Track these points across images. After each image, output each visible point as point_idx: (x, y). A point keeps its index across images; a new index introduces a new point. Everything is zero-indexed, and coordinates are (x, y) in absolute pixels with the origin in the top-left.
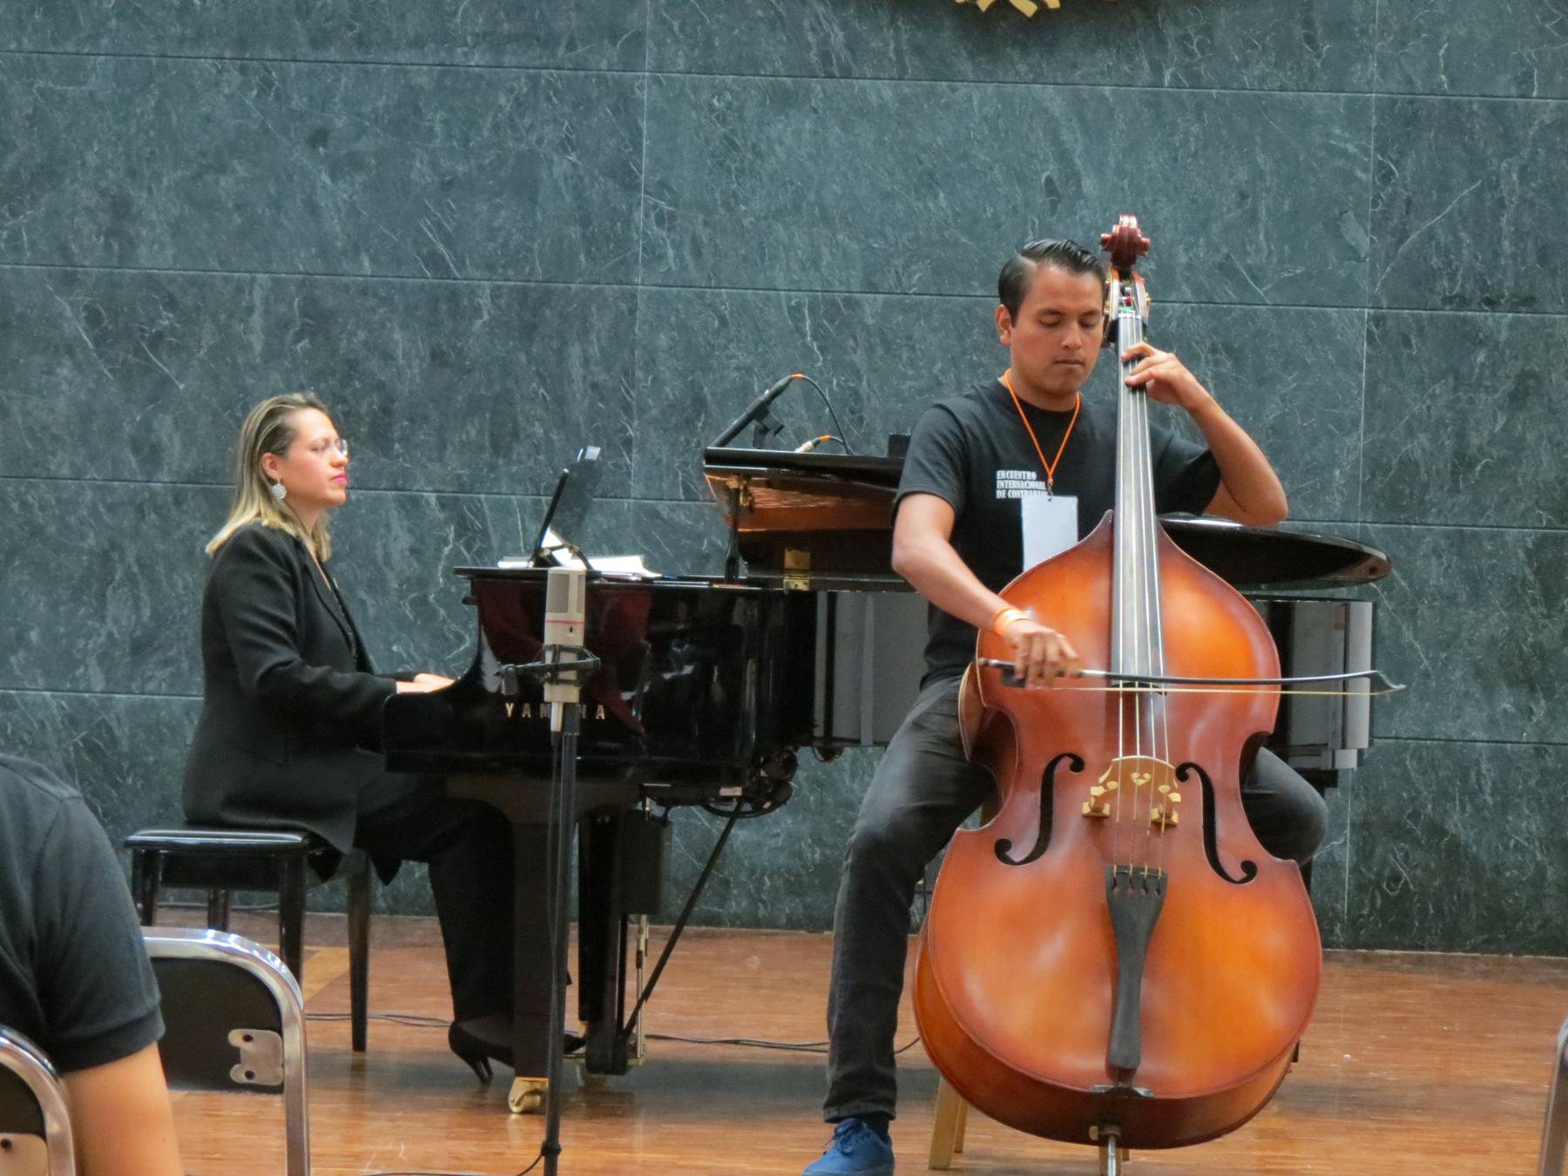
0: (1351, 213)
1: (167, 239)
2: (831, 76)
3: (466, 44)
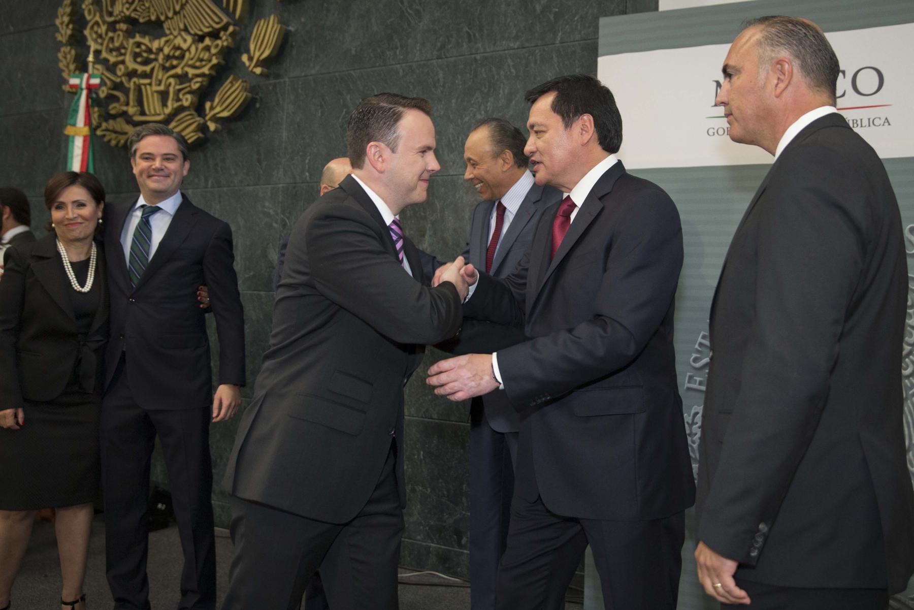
0: (271, 244)
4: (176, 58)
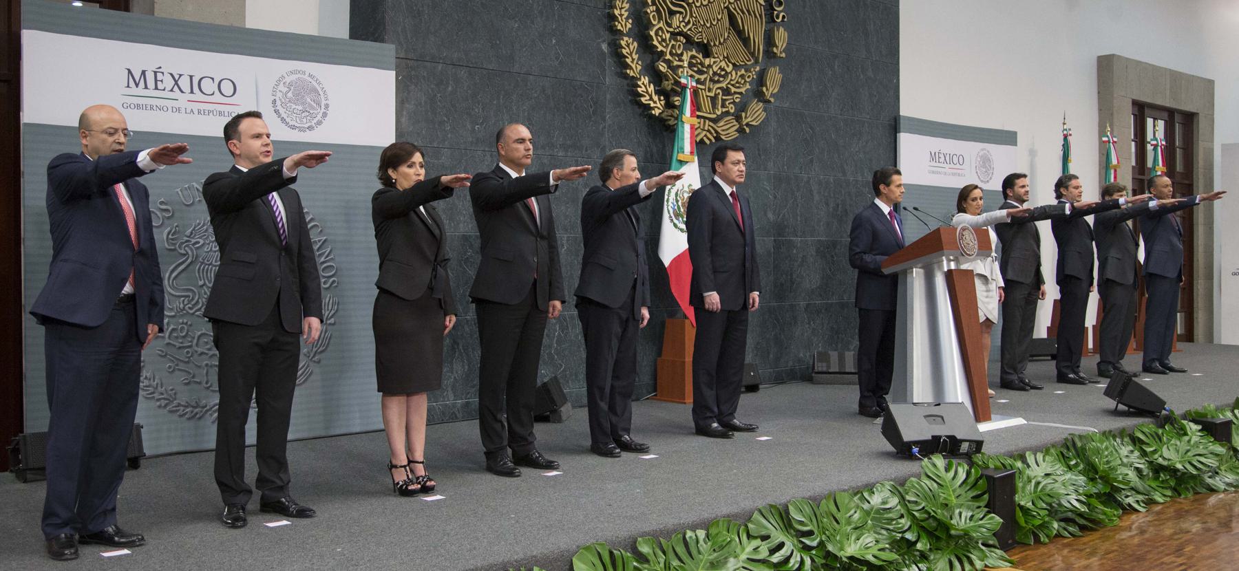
1: (469, 220)
2: (653, 163)
3: (557, 148)
4: (722, 76)
